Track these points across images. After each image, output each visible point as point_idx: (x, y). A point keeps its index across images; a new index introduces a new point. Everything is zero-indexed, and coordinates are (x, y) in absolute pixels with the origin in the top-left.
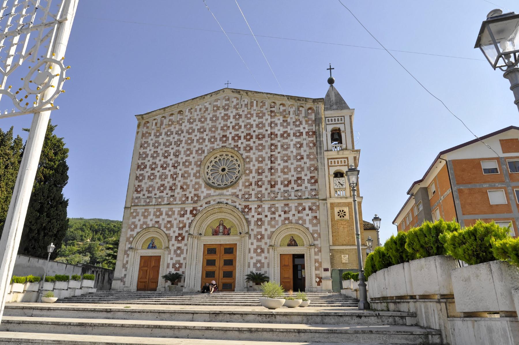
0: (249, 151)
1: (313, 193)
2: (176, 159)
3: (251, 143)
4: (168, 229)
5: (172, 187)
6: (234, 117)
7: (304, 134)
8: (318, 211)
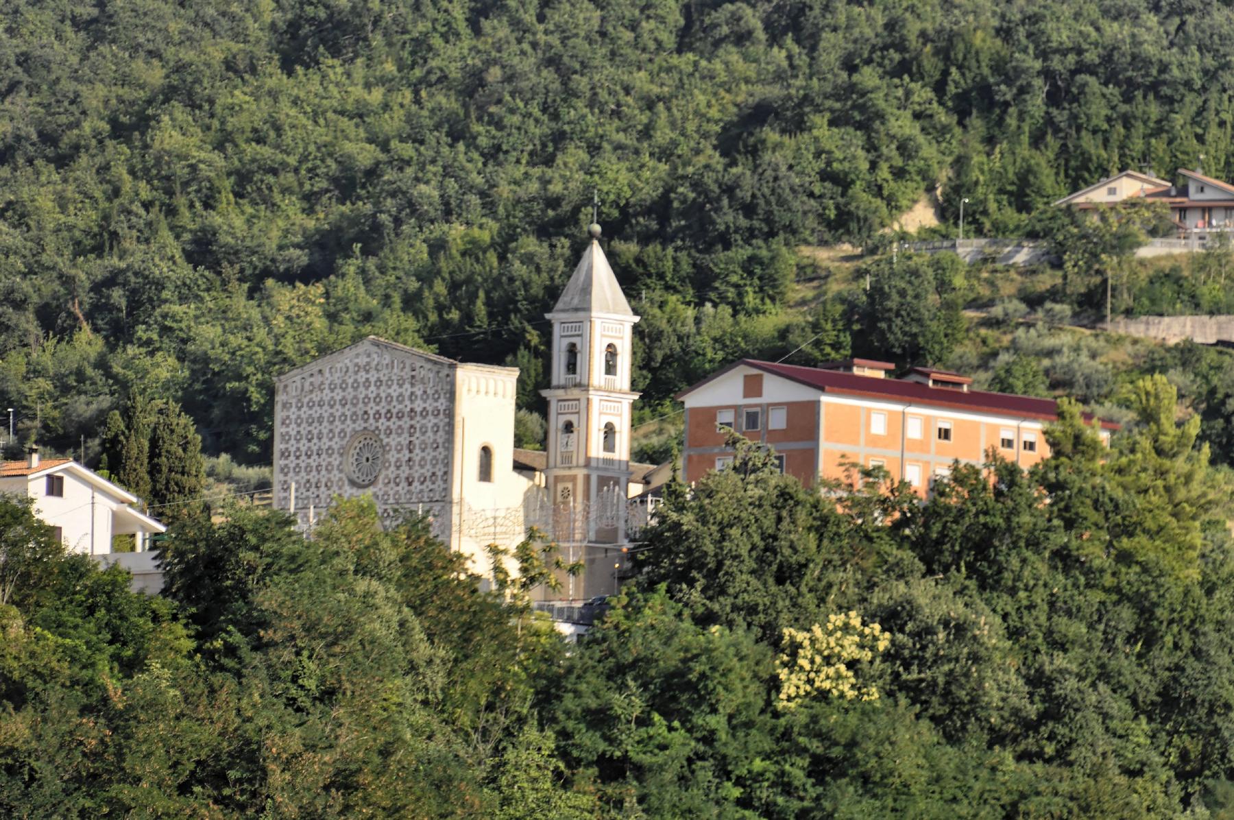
0: (388, 436)
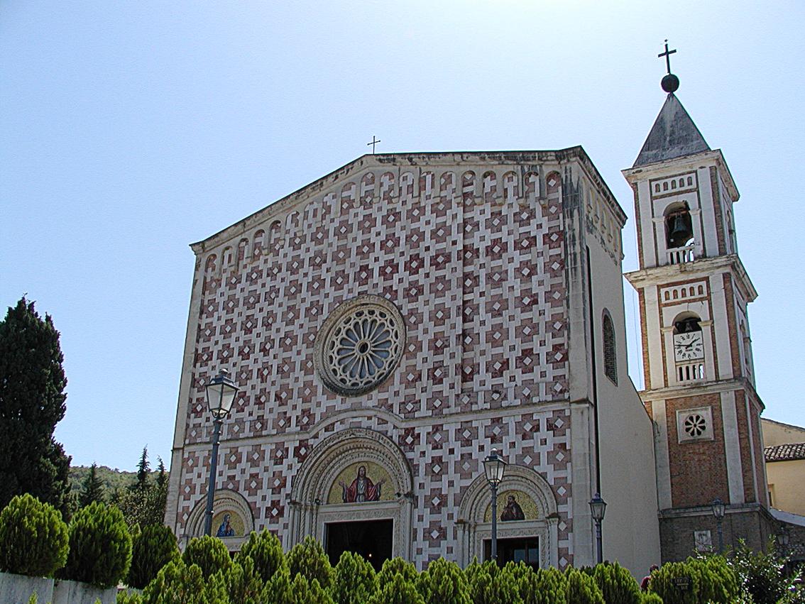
0: (414, 299)
1: (558, 387)
2: (267, 334)
3: (420, 277)
4: (253, 492)
5: (260, 397)
6: (385, 220)
7: (540, 241)
8: (568, 431)
